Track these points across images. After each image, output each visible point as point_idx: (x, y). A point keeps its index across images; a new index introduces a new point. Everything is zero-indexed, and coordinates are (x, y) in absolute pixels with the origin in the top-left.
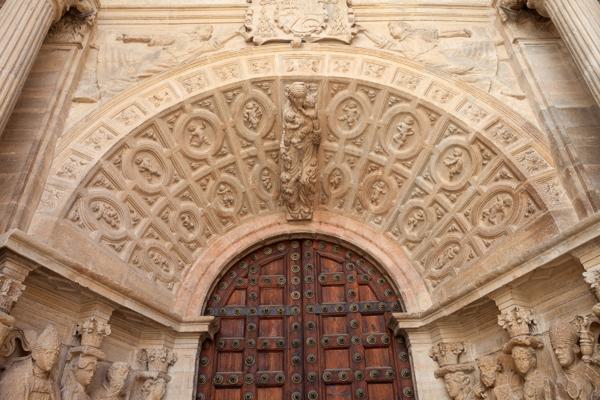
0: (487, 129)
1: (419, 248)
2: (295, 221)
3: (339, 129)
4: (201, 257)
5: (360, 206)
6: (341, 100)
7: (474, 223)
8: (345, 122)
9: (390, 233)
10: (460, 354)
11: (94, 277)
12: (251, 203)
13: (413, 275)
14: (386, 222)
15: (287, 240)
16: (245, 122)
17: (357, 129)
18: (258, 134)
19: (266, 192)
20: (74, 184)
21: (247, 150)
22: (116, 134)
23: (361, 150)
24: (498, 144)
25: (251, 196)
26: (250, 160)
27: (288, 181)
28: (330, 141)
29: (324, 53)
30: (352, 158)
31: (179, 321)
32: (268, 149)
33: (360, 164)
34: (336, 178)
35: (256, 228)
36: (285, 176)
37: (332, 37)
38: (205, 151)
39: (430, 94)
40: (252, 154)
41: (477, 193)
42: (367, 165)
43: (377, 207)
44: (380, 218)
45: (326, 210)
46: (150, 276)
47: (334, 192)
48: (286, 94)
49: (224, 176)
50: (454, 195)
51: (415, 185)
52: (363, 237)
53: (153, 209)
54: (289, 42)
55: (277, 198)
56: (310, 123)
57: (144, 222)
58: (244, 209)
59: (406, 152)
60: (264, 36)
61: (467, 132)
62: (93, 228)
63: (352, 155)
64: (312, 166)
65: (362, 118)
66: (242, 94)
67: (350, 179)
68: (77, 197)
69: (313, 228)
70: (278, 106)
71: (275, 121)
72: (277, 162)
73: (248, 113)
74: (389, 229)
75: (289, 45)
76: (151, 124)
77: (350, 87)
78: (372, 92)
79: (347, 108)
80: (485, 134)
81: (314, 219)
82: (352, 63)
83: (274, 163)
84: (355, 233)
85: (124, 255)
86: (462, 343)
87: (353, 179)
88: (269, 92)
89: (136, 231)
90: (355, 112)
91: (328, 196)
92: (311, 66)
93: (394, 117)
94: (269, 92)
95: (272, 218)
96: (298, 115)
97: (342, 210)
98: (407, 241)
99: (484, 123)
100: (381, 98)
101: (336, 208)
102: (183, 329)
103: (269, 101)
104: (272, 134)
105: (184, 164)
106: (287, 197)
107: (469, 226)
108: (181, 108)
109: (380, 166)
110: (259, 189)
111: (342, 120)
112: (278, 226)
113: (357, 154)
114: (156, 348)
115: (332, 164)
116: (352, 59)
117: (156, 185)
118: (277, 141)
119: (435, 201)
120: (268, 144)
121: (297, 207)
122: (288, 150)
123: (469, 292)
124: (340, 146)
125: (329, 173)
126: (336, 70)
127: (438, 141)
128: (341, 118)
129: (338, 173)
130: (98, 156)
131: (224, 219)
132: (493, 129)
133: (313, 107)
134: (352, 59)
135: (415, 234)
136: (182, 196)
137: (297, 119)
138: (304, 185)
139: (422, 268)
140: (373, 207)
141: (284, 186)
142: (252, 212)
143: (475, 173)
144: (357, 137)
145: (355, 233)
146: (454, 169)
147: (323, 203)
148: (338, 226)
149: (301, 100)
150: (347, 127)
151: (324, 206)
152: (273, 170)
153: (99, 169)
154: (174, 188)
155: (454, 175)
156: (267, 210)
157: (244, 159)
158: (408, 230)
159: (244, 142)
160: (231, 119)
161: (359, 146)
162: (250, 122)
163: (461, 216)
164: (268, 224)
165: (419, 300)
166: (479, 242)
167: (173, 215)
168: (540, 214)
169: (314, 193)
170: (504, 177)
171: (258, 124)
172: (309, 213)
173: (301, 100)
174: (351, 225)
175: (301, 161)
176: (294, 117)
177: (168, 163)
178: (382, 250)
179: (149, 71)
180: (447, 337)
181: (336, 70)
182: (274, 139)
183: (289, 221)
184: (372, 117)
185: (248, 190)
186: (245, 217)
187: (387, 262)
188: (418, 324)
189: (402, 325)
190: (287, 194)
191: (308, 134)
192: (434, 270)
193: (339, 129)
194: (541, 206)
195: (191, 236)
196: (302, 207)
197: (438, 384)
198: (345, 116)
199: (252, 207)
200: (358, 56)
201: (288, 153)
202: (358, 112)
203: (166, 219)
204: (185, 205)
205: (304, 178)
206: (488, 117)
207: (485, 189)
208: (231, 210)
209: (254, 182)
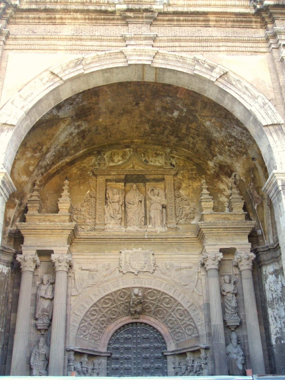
0: (189, 307)
1: (172, 330)
2: (135, 319)
4: (107, 331)
5: (156, 314)
7: (185, 329)
9: (164, 324)
10: (180, 363)
11: (86, 350)
13: (170, 338)
14: (163, 320)
15: (132, 323)
17: (154, 298)
20: (77, 325)
22: (86, 308)
24: (191, 313)
25: (121, 312)
31: (101, 353)
33: (155, 306)
36: (131, 309)
37: (147, 271)
38: (108, 305)
39: (175, 294)
41: (186, 323)
46: (93, 341)
47: (147, 310)
49: (113, 309)
50: (181, 321)
51: (171, 314)
52: (156, 324)
53: (94, 324)
54: (134, 273)
57: (92, 327)
59: (168, 306)
60: (126, 270)
61: (183, 307)
62: (81, 334)
65: (155, 296)
68: (79, 328)
69: (141, 320)
74: (164, 322)
76: (95, 304)
80: (188, 310)
81: (141, 317)
85: (87, 339)
86: (180, 360)
87: (153, 308)
89: (90, 331)
93: (164, 298)
95: (127, 318)
98: (169, 327)
99: (189, 304)
100: (160, 294)
102: (102, 355)
105: (102, 310)
107: (184, 331)
108: (103, 298)
109: (160, 307)
114: (96, 361)
115: (147, 304)
117: (95, 317)
118: (130, 300)
119: (176, 320)
120: (126, 301)
123: (180, 350)
127: (177, 306)
130: (82, 316)
131: (111, 319)
132: (191, 307)
135: (171, 326)
136: (101, 317)
139: (173, 336)
140: (159, 316)
143: (185, 317)
146: (181, 314)
148: (148, 320)
153: (83, 319)
154: (100, 316)
155: (181, 316)
158: (169, 324)
163: (182, 326)
164: (126, 320)
165: (171, 347)
166: (186, 336)
167: (99, 322)
168: (197, 335)
170: (191, 322)
174: (152, 319)
177: (98, 311)
178: (161, 328)
179: (92, 285)
180: (178, 359)
187: (162, 332)
188: (169, 354)
189: (165, 354)
192: (176, 338)
194: (198, 333)
195: (104, 326)
197: (173, 370)
203: (97, 325)
204: (101, 319)
205: (138, 310)
206: (190, 303)
207: (188, 323)
208: (115, 317)
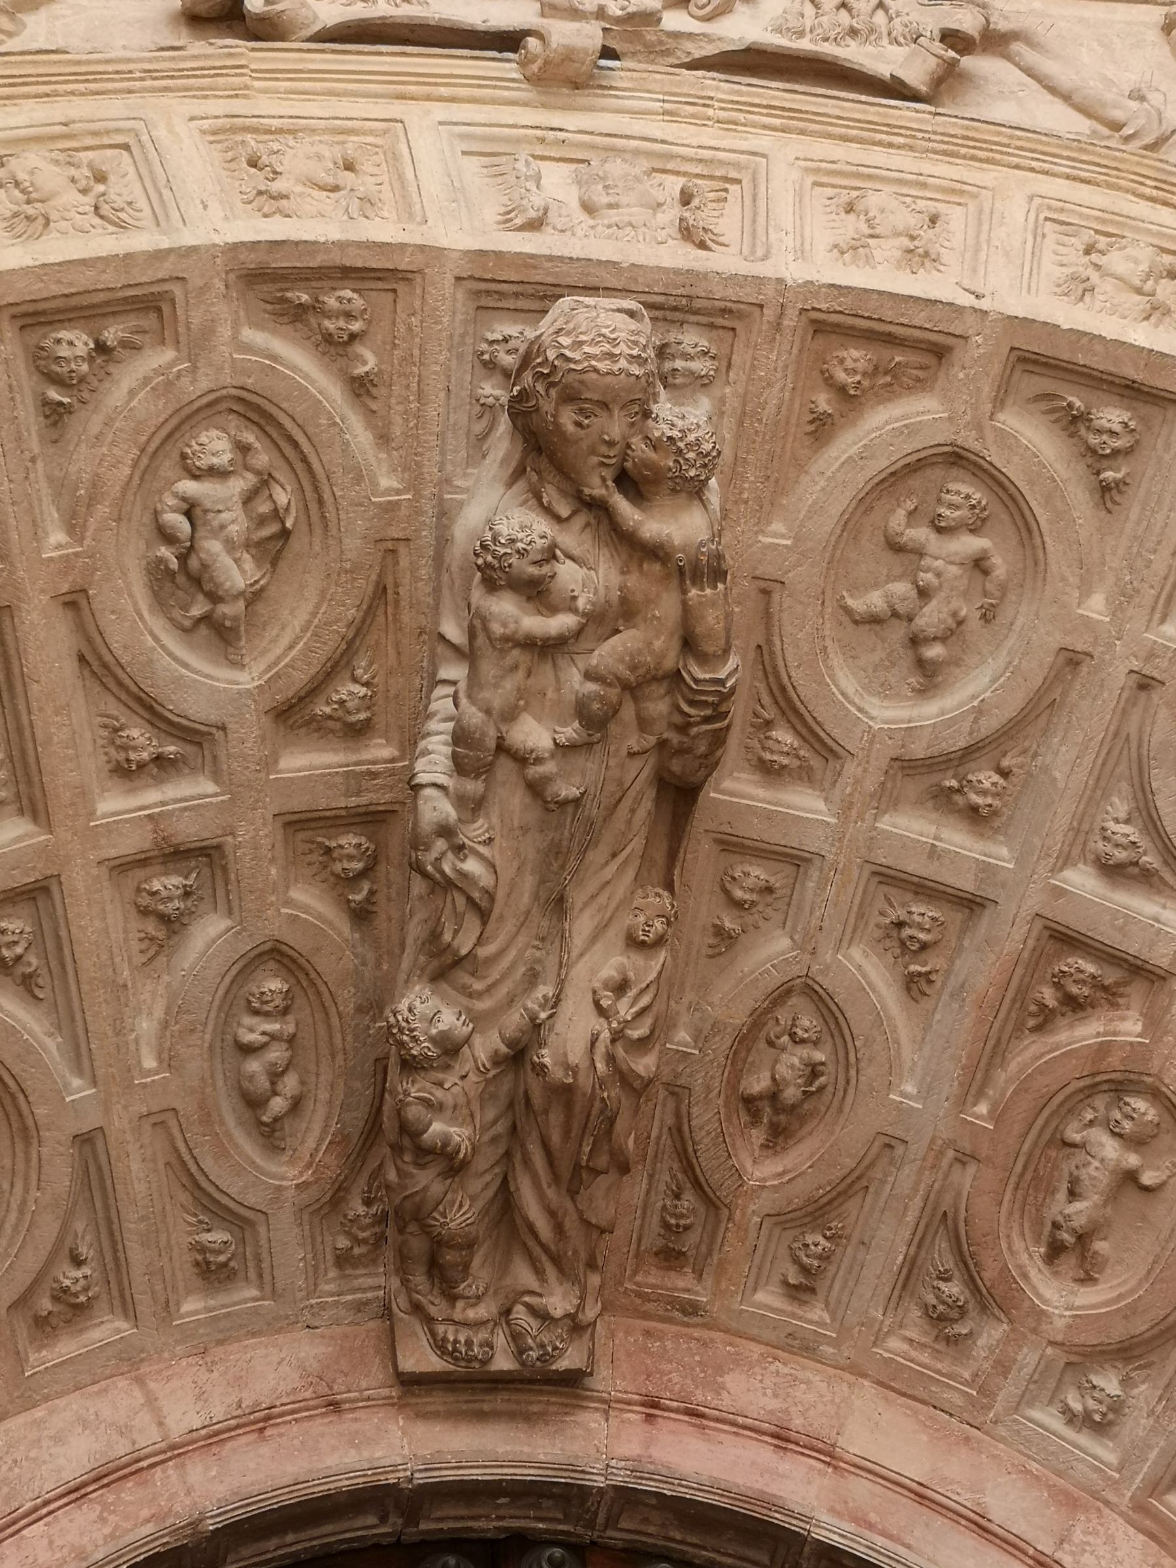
3: (847, 681)
6: (881, 464)
8: (897, 633)
12: (132, 1224)
16: (159, 575)
18: (247, 679)
19: (247, 1146)
21: (151, 796)
23: (1001, 854)
26: (168, 883)
27: (450, 1048)
28: (769, 771)
29: (762, 141)
30: (922, 911)
32: (299, 802)
34: (791, 1062)
35: (148, 1437)
40: (188, 831)
42: (1038, 959)
43: (1089, 1297)
44: (1109, 1383)
45: (691, 1309)
48: (492, 390)
55: (337, 1199)
56: (667, 607)
58: (70, 1276)
63: (924, 889)
64: (634, 943)
66: (159, 358)
67: (892, 1067)
70: (415, 484)
71: (381, 591)
72: (361, 915)
73: (191, 510)
75: (506, 67)
77: (961, 369)
78: (1112, 416)
79: (920, 534)
81: (603, 1381)
82: (956, 217)
83: (345, 925)
84: (921, 1496)
88: (368, 360)
90: (979, 565)
91: (711, 1202)
92: (671, 214)
94: (368, 360)
96: (570, 539)
97: (817, 1313)
101: (768, 1298)
103: (360, 435)
104: (348, 690)
106: (426, 1180)
110: (207, 1116)
111: (874, 620)
112: (323, 1427)
113: (966, 883)
116: (957, 192)
118: (380, 750)
121: (480, 1274)
122: (472, 806)
124: (845, 810)
125: (739, 1016)
126: (853, 250)
128: (875, 601)
129: (808, 1022)
133: (696, 491)
134: (957, 192)
137: (567, 574)
138: (564, 1093)
141: (416, 1089)
142: (128, 1309)
144: (969, 753)
145: (921, 1496)
147: (671, 1258)
149: (615, 426)
150: (905, 677)
151: (682, 1283)
152: (327, 966)
156: (245, 1294)
157: (122, 867)
159: (137, 733)
160: (57, 536)
161: (976, 817)
162: (196, 581)
169: (624, 1168)
171: (254, 597)
172: (576, 1326)
173: (615, 426)
175: (558, 905)
176: (550, 554)
181: (853, 250)
182: (357, 732)
183: (412, 1383)
184: (1096, 607)
185: (119, 1122)
186: (67, 1347)
190: (425, 1154)
191: (634, 685)
193: (847, 681)
196: (524, 1276)
198: (901, 588)
199: (137, 1255)
200: (989, 176)
201: (475, 831)
202: (1000, 566)
209: (169, 1060)
